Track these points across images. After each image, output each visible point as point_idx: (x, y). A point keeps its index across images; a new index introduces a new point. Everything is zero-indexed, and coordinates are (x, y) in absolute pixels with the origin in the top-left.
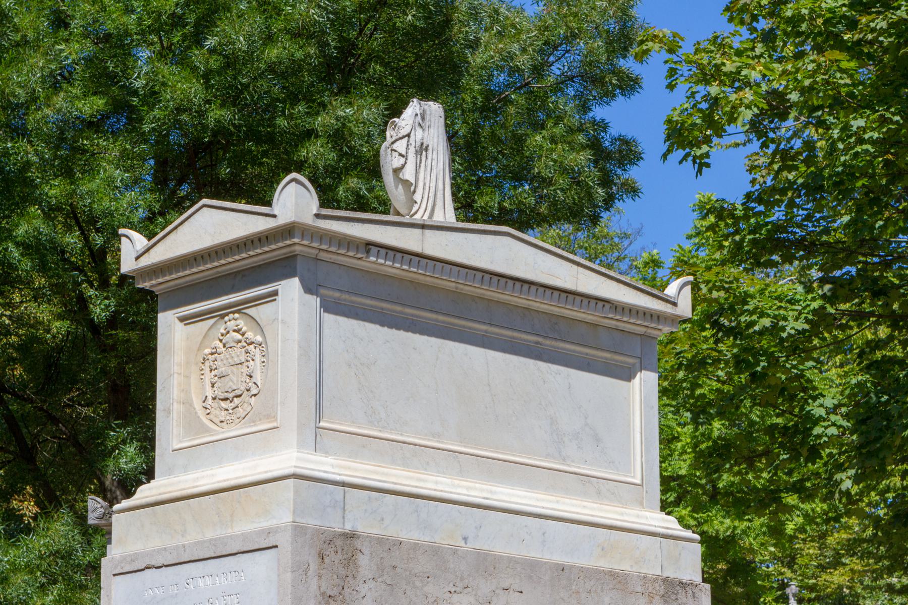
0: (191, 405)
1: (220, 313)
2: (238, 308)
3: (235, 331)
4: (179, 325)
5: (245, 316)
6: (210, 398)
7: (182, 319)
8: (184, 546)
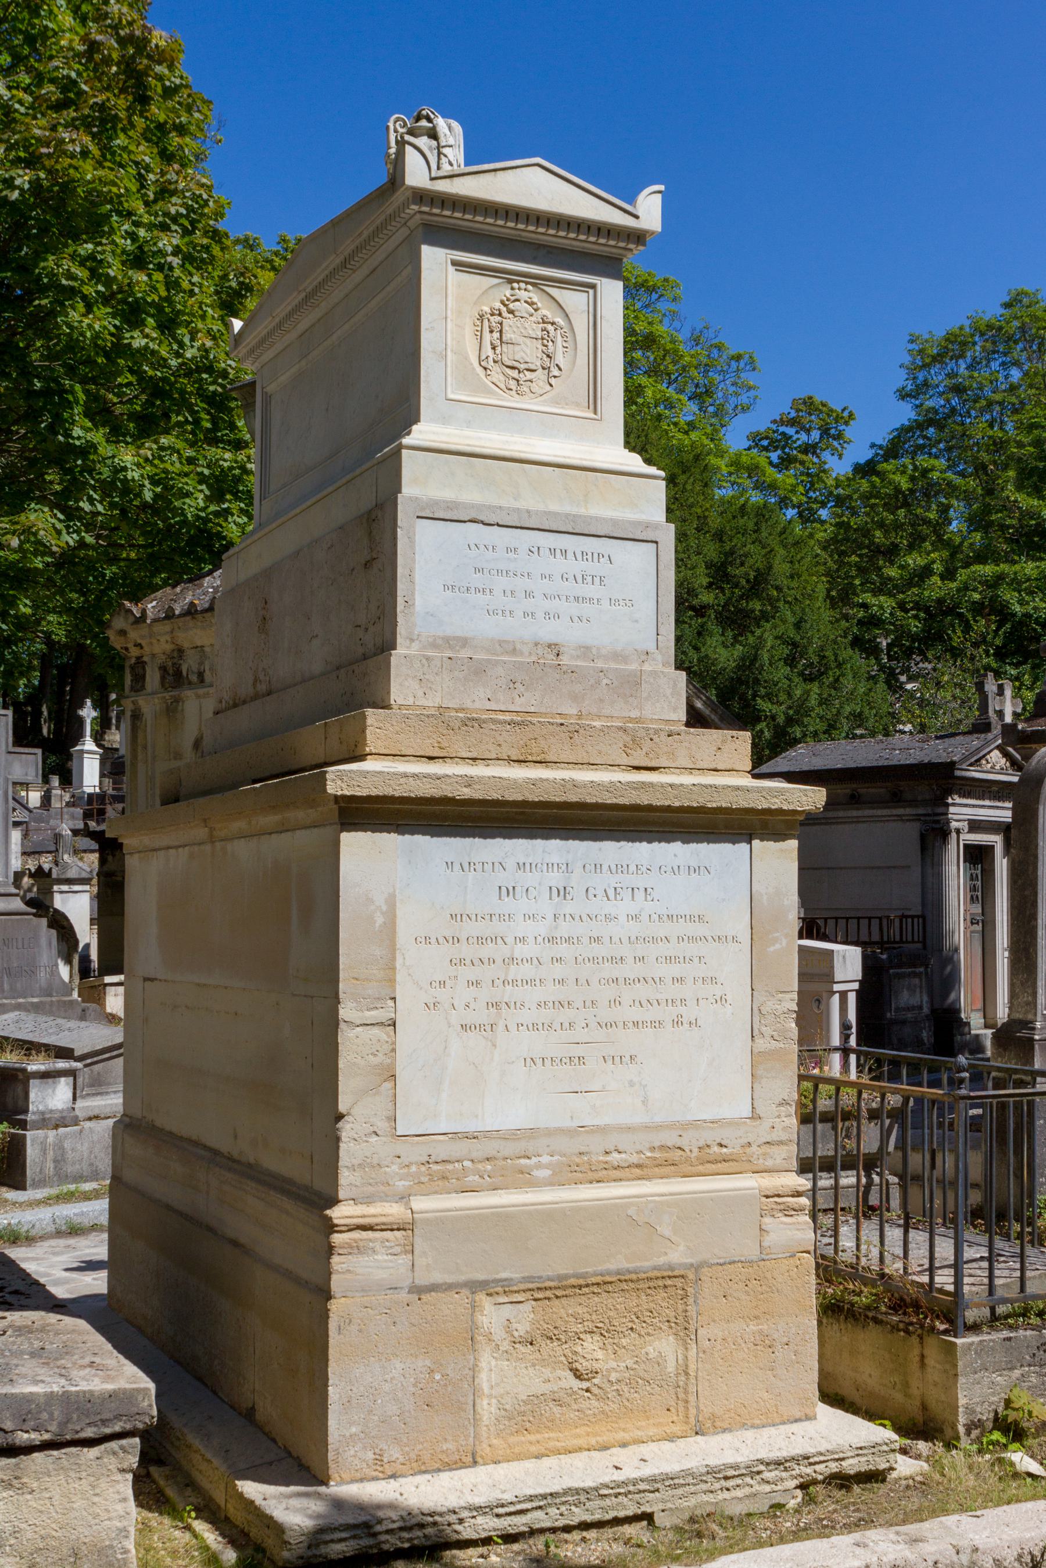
0: (467, 358)
1: (511, 278)
2: (536, 282)
3: (526, 302)
4: (451, 269)
5: (540, 292)
6: (491, 360)
7: (454, 263)
8: (528, 512)
